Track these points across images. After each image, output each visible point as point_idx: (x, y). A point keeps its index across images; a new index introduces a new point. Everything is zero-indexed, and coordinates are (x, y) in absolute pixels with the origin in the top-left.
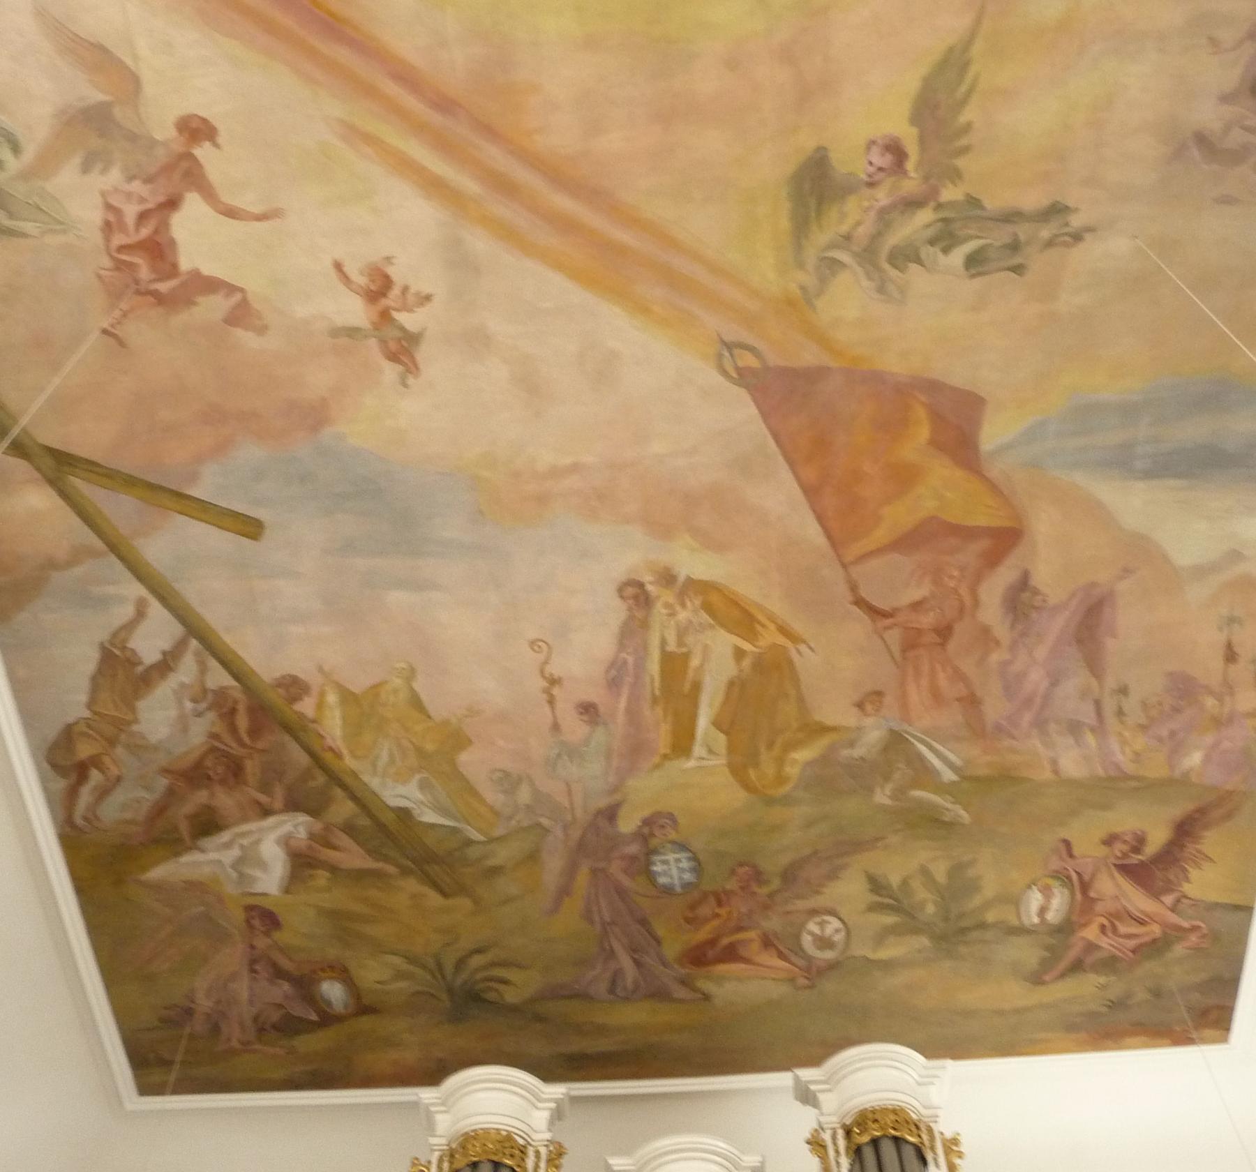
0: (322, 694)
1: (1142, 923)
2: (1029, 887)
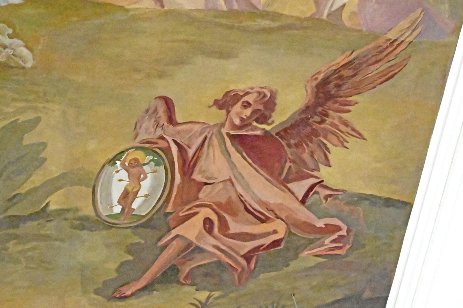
1: (264, 220)
2: (112, 162)
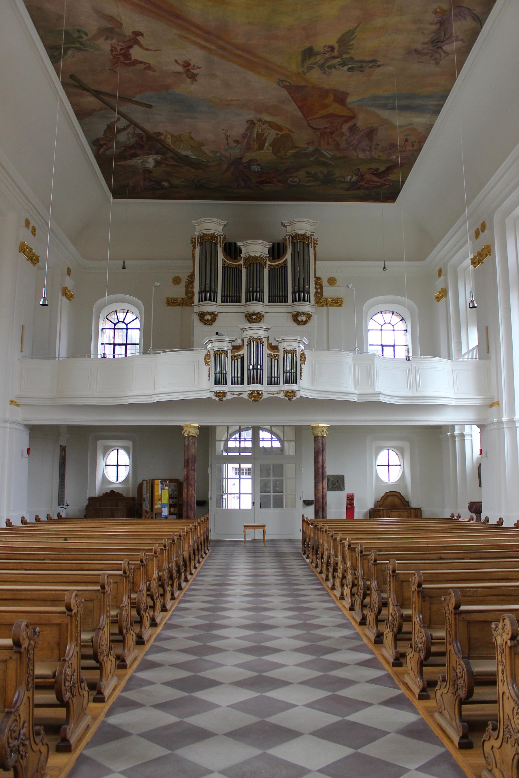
0: (166, 136)
